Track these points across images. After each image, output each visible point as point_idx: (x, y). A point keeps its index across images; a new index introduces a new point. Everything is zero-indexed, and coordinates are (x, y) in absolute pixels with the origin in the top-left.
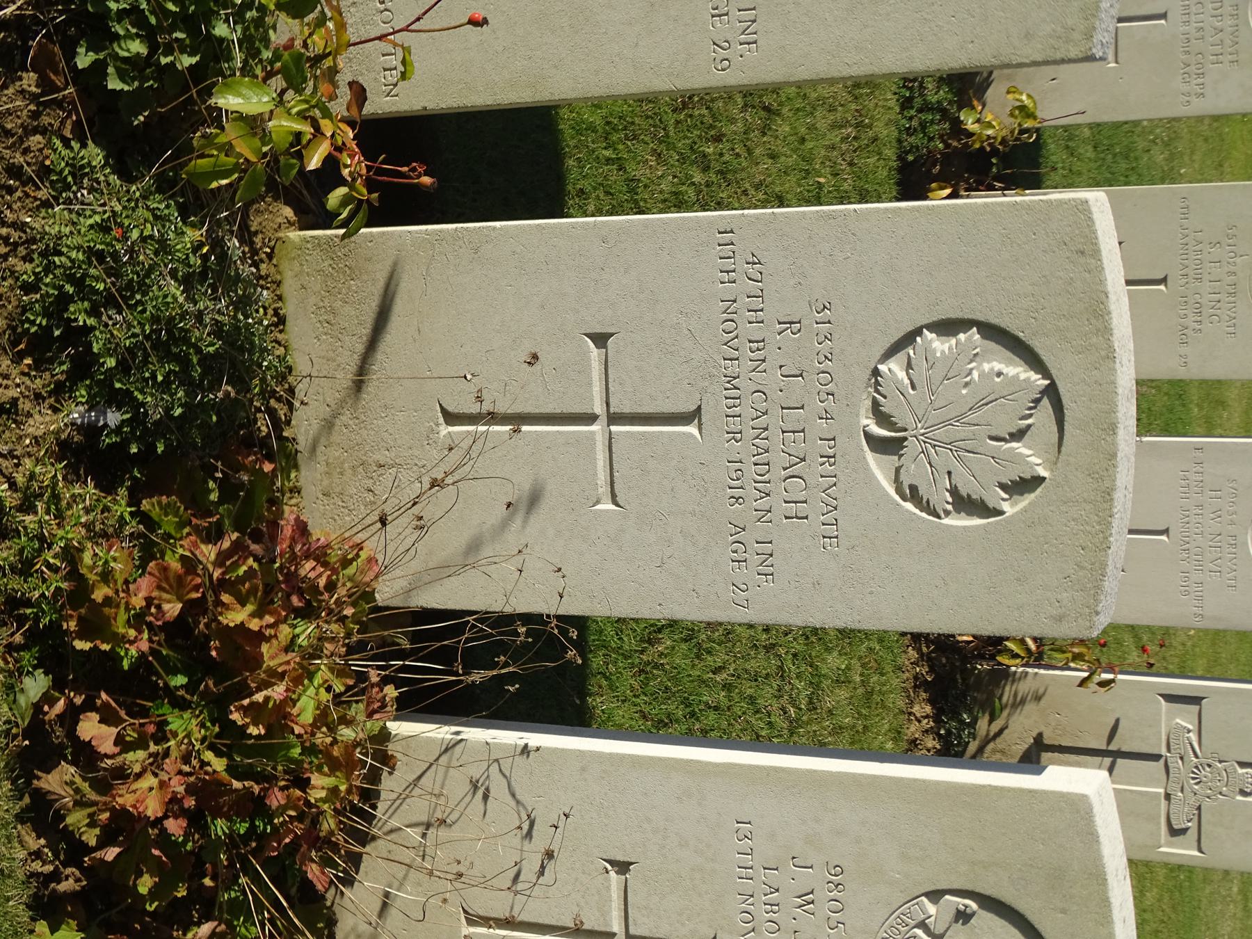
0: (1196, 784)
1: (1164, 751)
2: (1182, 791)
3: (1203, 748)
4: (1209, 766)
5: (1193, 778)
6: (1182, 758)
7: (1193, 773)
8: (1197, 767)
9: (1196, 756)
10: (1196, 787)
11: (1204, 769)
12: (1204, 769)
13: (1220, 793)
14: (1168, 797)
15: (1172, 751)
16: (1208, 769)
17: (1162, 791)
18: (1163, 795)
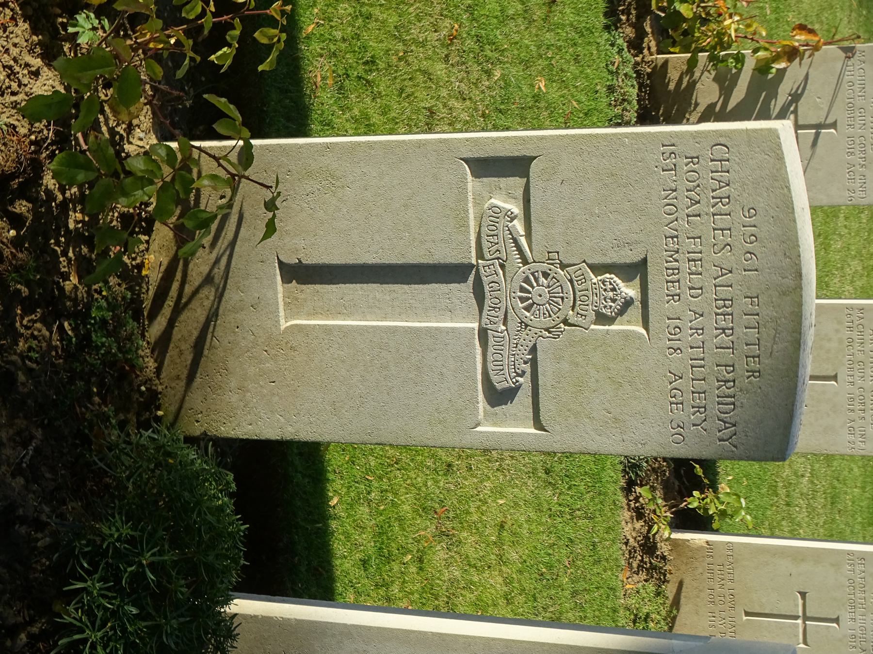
0: (528, 309)
1: (474, 262)
2: (505, 324)
3: (534, 252)
4: (546, 275)
5: (523, 300)
6: (502, 266)
7: (522, 290)
8: (527, 280)
9: (525, 262)
10: (528, 314)
11: (536, 280)
12: (536, 280)
13: (565, 322)
14: (483, 334)
15: (487, 256)
16: (542, 280)
17: (476, 325)
18: (477, 329)
